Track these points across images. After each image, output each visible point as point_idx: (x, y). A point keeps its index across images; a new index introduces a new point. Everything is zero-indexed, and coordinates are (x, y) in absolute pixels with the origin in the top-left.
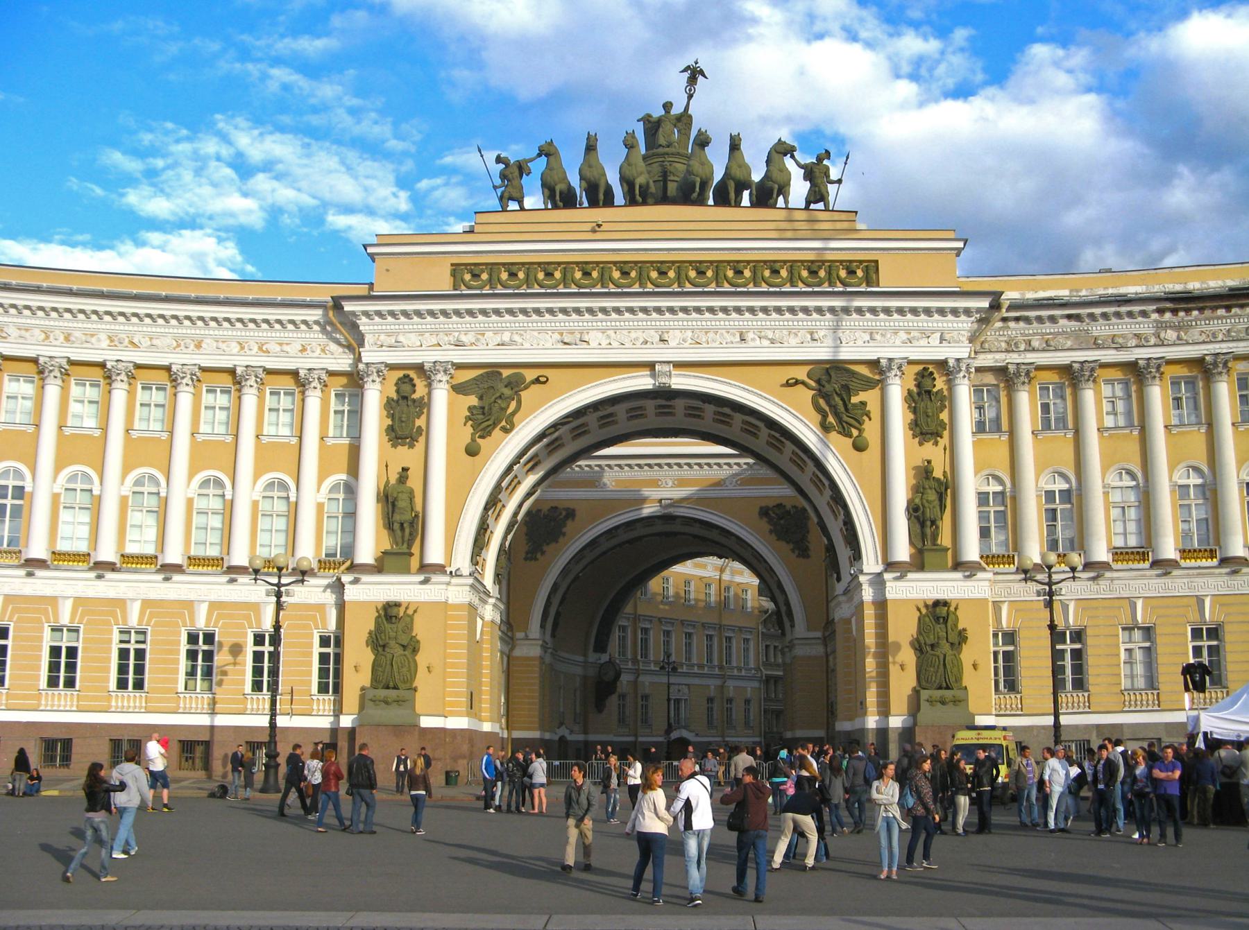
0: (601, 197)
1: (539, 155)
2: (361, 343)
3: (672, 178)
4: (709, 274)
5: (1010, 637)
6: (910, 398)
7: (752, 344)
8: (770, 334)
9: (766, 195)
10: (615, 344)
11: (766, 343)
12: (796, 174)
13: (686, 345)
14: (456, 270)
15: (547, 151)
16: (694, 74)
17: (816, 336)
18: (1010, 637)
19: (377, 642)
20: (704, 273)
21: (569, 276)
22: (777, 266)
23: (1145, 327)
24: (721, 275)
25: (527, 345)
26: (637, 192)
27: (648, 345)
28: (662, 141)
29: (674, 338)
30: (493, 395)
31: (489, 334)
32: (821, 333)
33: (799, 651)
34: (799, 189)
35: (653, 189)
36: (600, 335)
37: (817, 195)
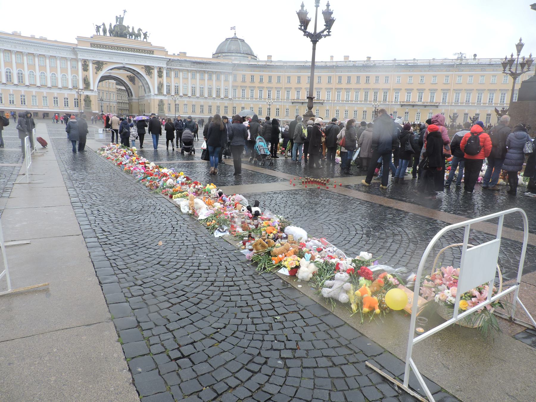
2: (77, 54)
5: (170, 104)
6: (158, 72)
9: (138, 35)
12: (142, 35)
14: (91, 44)
15: (104, 24)
16: (125, 11)
18: (170, 104)
19: (85, 100)
23: (189, 65)
29: (126, 60)
30: (99, 65)
33: (134, 101)
34: (142, 36)
37: (145, 38)
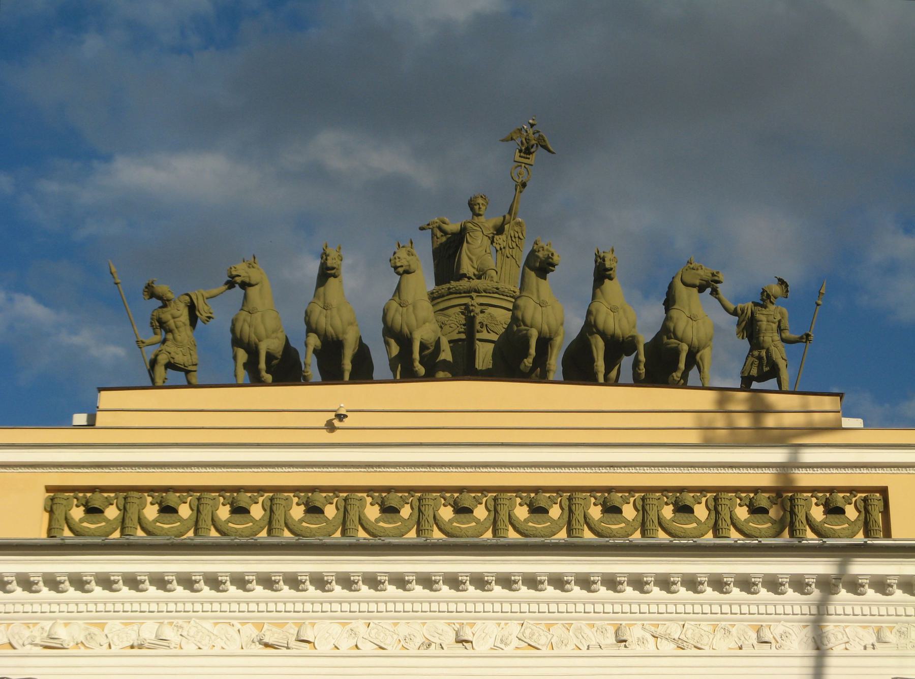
0: (348, 365)
1: (231, 284)
3: (484, 335)
4: (555, 512)
7: (639, 650)
8: (675, 631)
10: (367, 648)
11: (668, 647)
13: (509, 650)
17: (767, 636)
20: (545, 511)
21: (279, 514)
22: (688, 498)
24: (579, 515)
25: (190, 648)
26: (416, 355)
27: (433, 650)
28: (467, 267)
31: (114, 626)
32: (778, 629)
35: (446, 355)
36: (336, 628)
